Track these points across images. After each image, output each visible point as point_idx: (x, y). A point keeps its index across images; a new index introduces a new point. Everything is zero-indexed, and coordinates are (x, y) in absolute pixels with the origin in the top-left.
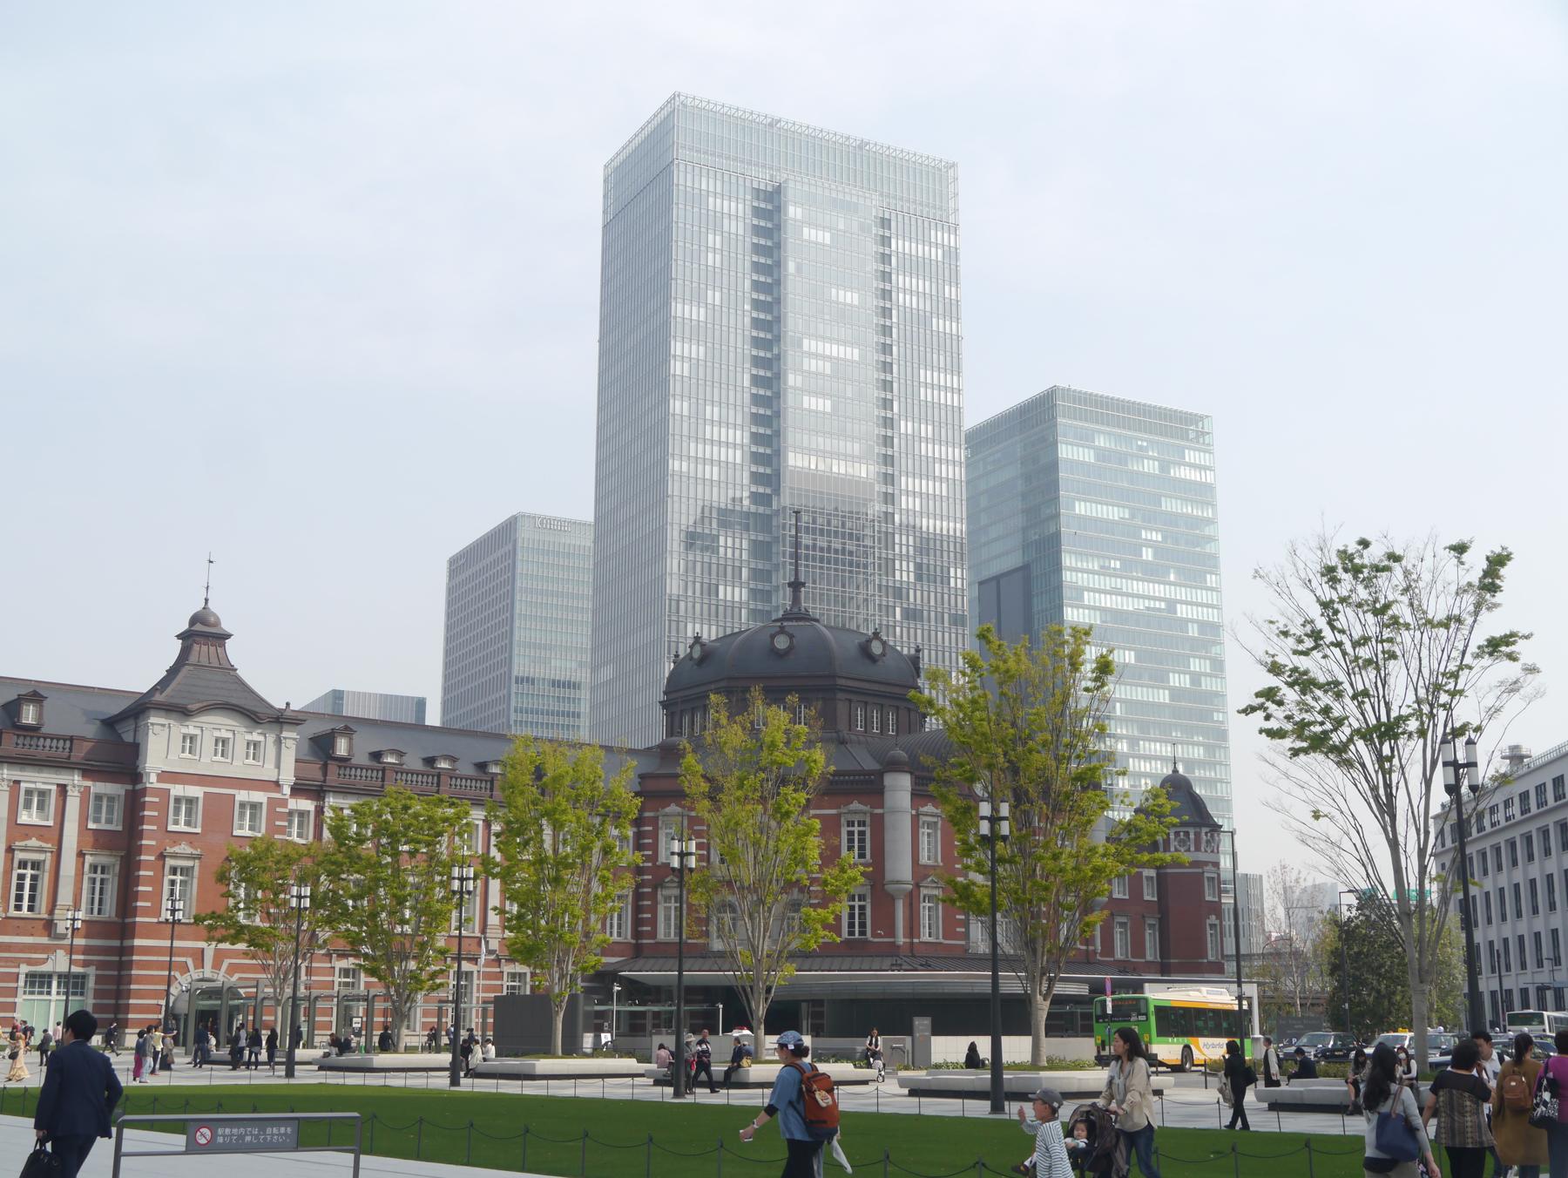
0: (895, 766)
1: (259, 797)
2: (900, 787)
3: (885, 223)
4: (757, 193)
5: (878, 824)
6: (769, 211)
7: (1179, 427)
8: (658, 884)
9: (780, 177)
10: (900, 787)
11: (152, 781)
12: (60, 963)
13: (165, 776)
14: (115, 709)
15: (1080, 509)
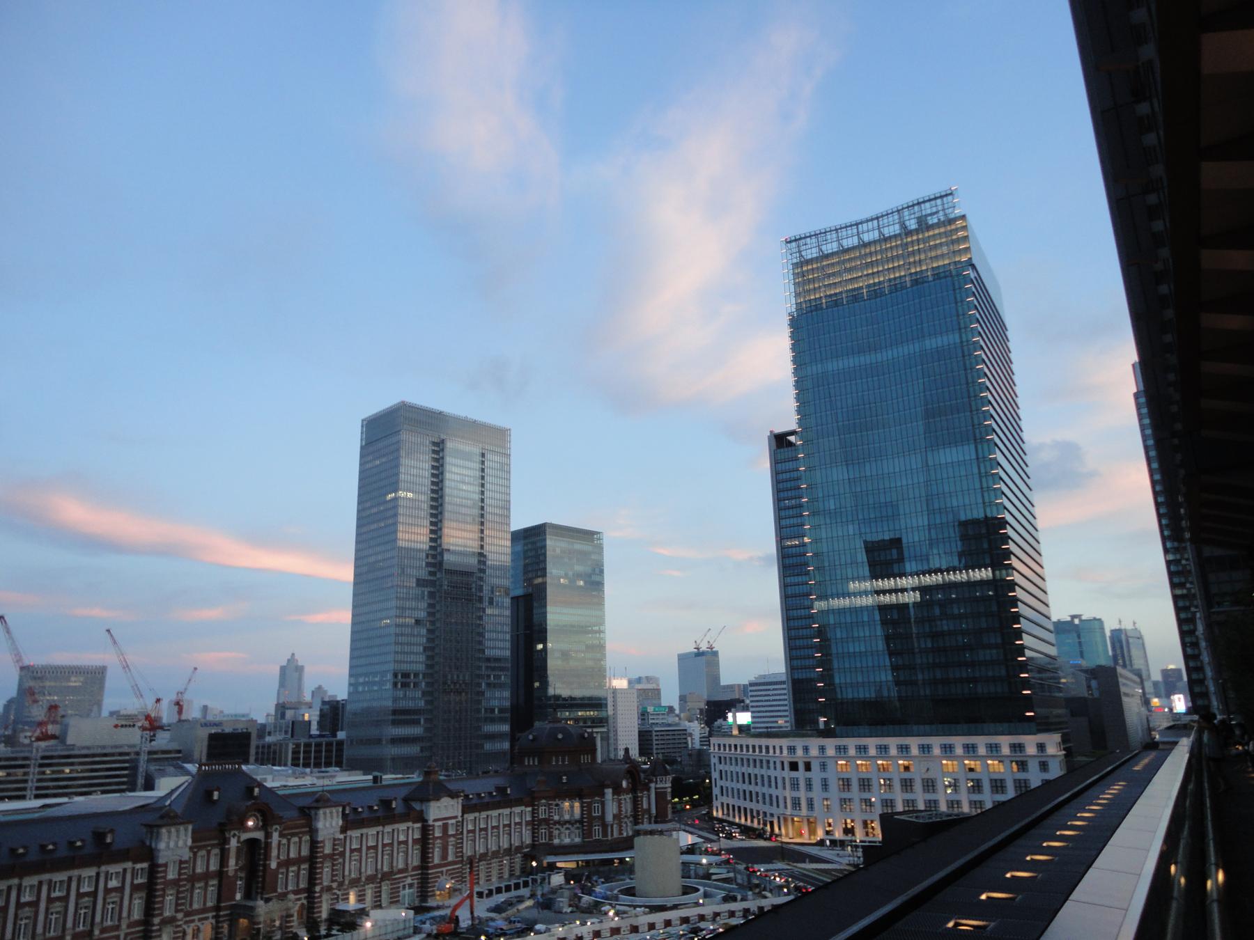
0: (608, 787)
1: (453, 821)
2: (609, 792)
3: (483, 455)
4: (434, 444)
5: (603, 804)
6: (439, 449)
7: (589, 536)
8: (539, 825)
9: (443, 437)
10: (609, 792)
11: (431, 823)
12: (409, 880)
13: (435, 820)
14: (404, 792)
15: (553, 570)
